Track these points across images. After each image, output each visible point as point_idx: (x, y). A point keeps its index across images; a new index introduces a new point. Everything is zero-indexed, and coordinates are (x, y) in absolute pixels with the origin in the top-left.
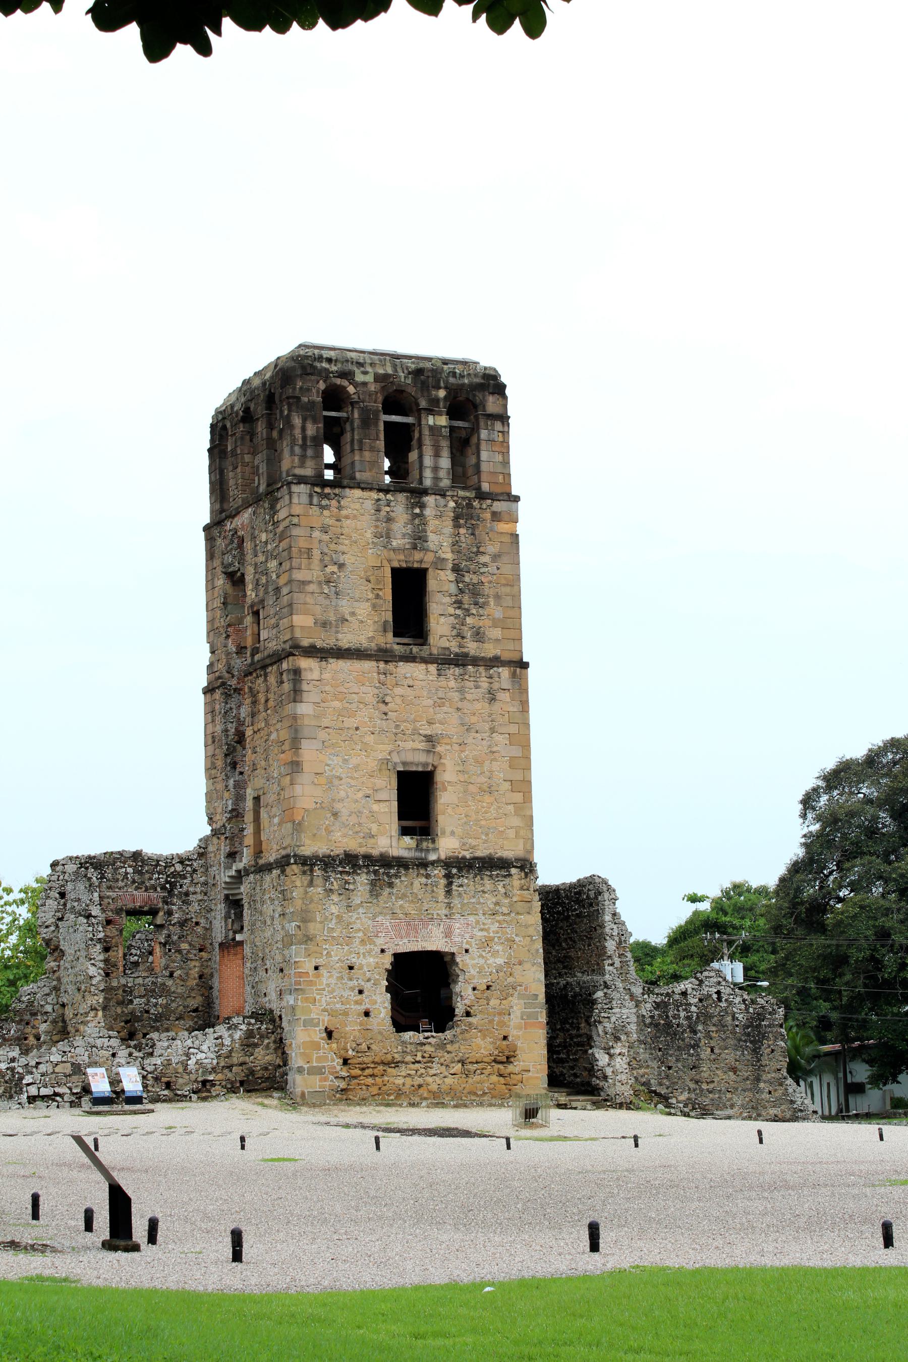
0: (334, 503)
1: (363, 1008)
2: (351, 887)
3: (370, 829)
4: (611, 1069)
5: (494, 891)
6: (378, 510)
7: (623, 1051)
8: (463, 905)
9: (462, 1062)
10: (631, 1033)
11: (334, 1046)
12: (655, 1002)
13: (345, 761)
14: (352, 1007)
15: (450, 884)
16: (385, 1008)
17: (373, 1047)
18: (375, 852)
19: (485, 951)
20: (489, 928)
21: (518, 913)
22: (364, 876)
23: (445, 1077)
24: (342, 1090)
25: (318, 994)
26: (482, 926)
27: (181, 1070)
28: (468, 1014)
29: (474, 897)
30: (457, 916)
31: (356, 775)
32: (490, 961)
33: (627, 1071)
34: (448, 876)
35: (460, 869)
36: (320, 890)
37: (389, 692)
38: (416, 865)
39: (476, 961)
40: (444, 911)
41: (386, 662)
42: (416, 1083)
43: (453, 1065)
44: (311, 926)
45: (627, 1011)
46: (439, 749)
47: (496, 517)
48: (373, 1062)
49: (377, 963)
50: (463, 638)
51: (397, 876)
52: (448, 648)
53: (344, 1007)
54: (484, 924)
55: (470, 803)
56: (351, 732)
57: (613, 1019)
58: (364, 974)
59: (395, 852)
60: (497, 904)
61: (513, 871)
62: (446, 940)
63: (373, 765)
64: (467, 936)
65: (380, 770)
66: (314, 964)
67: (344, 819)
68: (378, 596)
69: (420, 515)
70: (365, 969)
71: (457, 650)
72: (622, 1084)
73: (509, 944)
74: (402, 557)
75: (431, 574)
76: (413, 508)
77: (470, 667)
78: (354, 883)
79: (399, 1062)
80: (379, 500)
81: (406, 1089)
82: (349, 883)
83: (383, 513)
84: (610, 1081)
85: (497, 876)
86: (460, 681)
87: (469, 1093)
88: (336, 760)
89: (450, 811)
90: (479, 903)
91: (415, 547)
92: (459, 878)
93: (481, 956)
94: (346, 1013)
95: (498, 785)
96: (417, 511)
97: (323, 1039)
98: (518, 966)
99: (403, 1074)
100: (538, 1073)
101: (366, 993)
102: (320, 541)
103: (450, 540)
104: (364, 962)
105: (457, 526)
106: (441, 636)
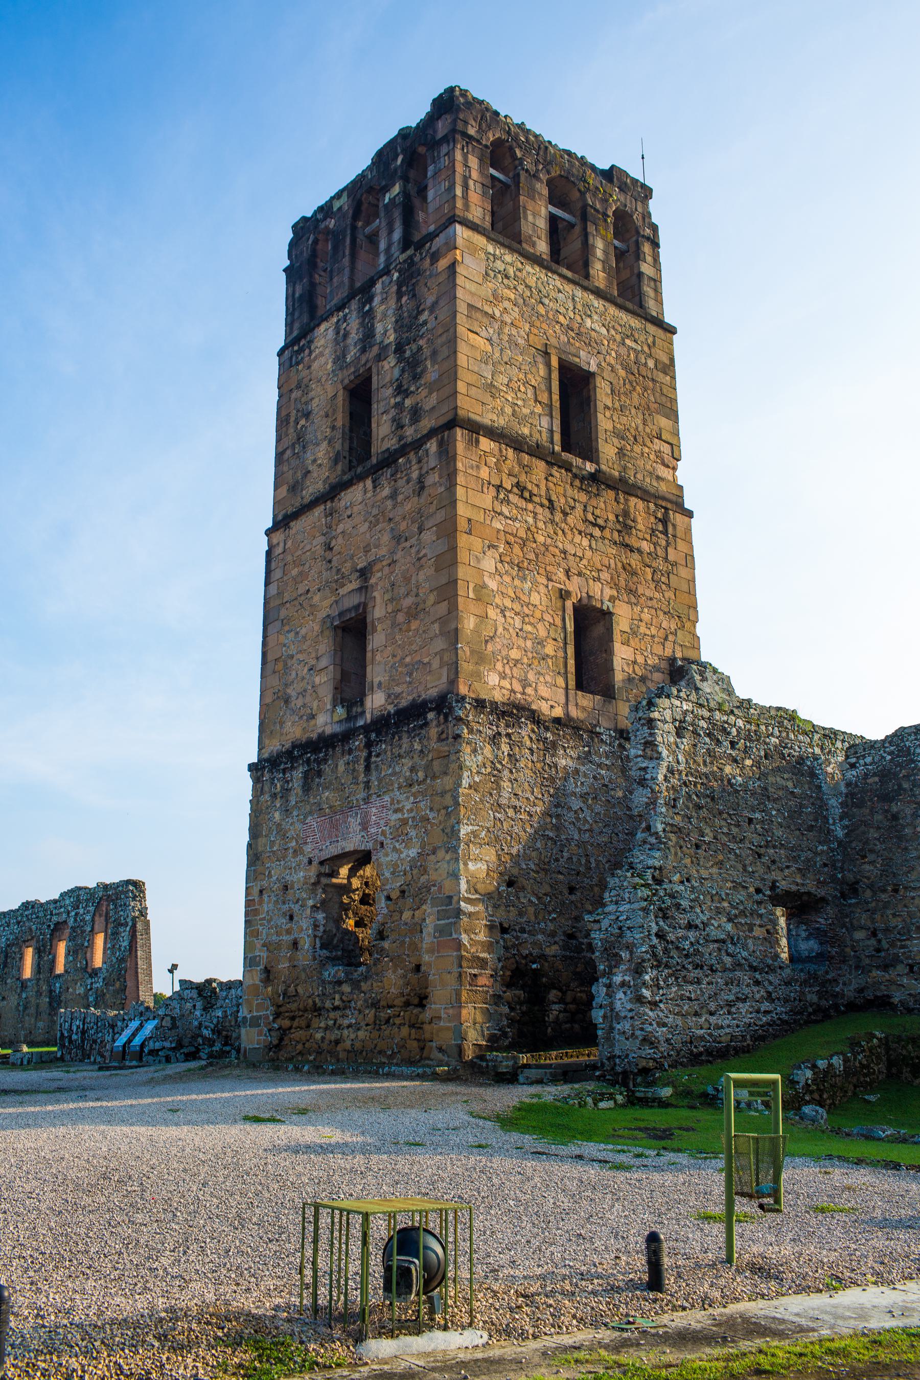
0: (307, 351)
1: (292, 937)
2: (290, 785)
3: (311, 709)
4: (601, 1013)
6: (338, 333)
7: (627, 978)
8: (380, 780)
9: (375, 1005)
10: (635, 945)
11: (270, 989)
13: (297, 633)
15: (370, 755)
16: (308, 936)
18: (314, 736)
19: (398, 841)
20: (403, 806)
21: (434, 777)
22: (301, 769)
23: (358, 1029)
24: (276, 1046)
25: (261, 925)
26: (397, 806)
27: (233, 1023)
29: (390, 766)
31: (305, 647)
32: (402, 856)
33: (630, 1014)
34: (369, 745)
35: (378, 734)
36: (267, 797)
37: (334, 533)
38: (339, 741)
39: (389, 859)
40: (362, 795)
41: (332, 499)
42: (333, 1038)
43: (367, 1012)
44: (260, 839)
45: (628, 906)
46: (373, 581)
47: (435, 257)
48: (299, 1010)
49: (305, 877)
50: (402, 427)
51: (325, 760)
52: (388, 449)
53: (279, 938)
54: (398, 802)
55: (397, 637)
56: (303, 598)
57: (605, 924)
58: (295, 893)
59: (329, 730)
60: (413, 769)
61: (431, 715)
62: (363, 834)
63: (317, 628)
64: (382, 822)
65: (322, 632)
66: (259, 888)
67: (293, 704)
68: (333, 428)
69: (371, 309)
70: (296, 887)
71: (397, 446)
72: (627, 1039)
73: (424, 824)
74: (352, 370)
75: (374, 370)
76: (364, 306)
77: (400, 460)
78: (292, 780)
79: (320, 1009)
80: (338, 321)
81: (325, 1046)
82: (288, 782)
83: (342, 332)
84: (600, 1033)
85: (414, 729)
86: (393, 483)
87: (380, 1052)
88: (291, 635)
89: (378, 658)
90: (394, 774)
92: (377, 745)
93: (395, 849)
94: (279, 945)
95: (424, 602)
96: (367, 308)
98: (432, 857)
99: (322, 1025)
100: (449, 1021)
101: (295, 918)
102: (296, 400)
103: (394, 319)
104: (295, 878)
105: (399, 295)
106: (383, 439)
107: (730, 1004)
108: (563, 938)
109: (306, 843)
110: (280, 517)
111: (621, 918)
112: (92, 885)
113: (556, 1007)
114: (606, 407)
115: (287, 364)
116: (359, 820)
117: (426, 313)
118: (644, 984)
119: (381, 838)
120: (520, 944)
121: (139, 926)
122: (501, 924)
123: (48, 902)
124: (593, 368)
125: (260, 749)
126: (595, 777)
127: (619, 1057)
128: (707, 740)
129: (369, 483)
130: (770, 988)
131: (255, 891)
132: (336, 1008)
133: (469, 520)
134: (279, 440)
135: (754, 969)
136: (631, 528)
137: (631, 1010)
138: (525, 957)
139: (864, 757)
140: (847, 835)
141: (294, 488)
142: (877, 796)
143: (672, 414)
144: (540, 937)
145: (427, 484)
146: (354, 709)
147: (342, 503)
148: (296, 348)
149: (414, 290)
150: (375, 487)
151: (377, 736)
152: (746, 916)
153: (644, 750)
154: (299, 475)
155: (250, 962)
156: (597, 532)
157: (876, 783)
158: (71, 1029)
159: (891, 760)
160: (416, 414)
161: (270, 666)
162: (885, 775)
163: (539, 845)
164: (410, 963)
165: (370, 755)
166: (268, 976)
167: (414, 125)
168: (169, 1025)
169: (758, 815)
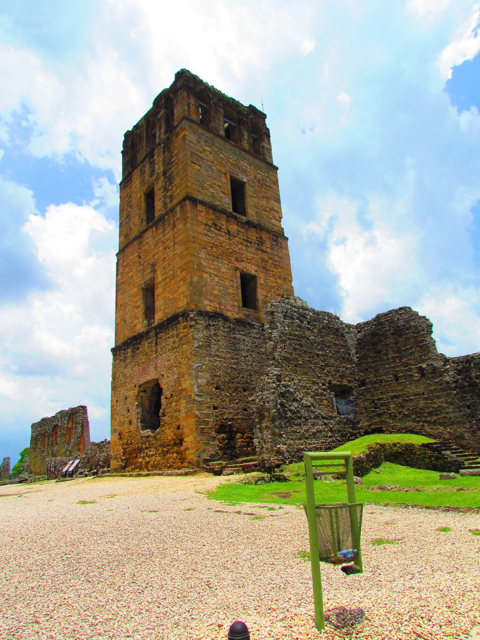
5: (173, 336)
7: (268, 424)
12: (456, 369)
14: (126, 420)
15: (157, 339)
17: (132, 441)
26: (168, 359)
28: (164, 415)
30: (159, 356)
33: (270, 440)
34: (156, 334)
60: (174, 343)
61: (180, 319)
62: (155, 372)
68: (140, 210)
69: (153, 160)
76: (151, 159)
77: (166, 217)
82: (126, 354)
91: (151, 176)
96: (152, 160)
97: (118, 439)
100: (193, 450)
107: (314, 434)
108: (242, 410)
109: (133, 378)
110: (121, 248)
111: (264, 398)
112: (67, 409)
113: (239, 440)
114: (251, 196)
115: (123, 188)
116: (153, 366)
117: (175, 157)
118: (276, 426)
119: (162, 373)
120: (222, 414)
121: (85, 424)
122: (214, 406)
123: (51, 417)
124: (245, 180)
125: (116, 342)
126: (252, 343)
127: (267, 460)
128: (297, 321)
129: (154, 229)
130: (331, 426)
131: (115, 401)
132: (147, 448)
133: (194, 237)
134: (120, 219)
135: (324, 418)
136: (263, 243)
137: (270, 439)
138: (225, 420)
139: (364, 328)
140: (358, 361)
141: (126, 236)
142: (370, 343)
143: (278, 201)
144: (231, 410)
145: (176, 224)
146: (151, 321)
147: (144, 238)
148: (126, 181)
149: (169, 149)
150: (156, 230)
151: (159, 330)
152: (319, 396)
153: (270, 325)
154: (128, 230)
155: (113, 431)
156: (249, 245)
157: (370, 338)
158: (50, 467)
159: (376, 327)
160: (171, 198)
161: (119, 307)
162: (373, 334)
163: (229, 371)
164: (175, 425)
165: (157, 339)
166: (120, 437)
167: (168, 87)
168: (87, 461)
169: (321, 353)
